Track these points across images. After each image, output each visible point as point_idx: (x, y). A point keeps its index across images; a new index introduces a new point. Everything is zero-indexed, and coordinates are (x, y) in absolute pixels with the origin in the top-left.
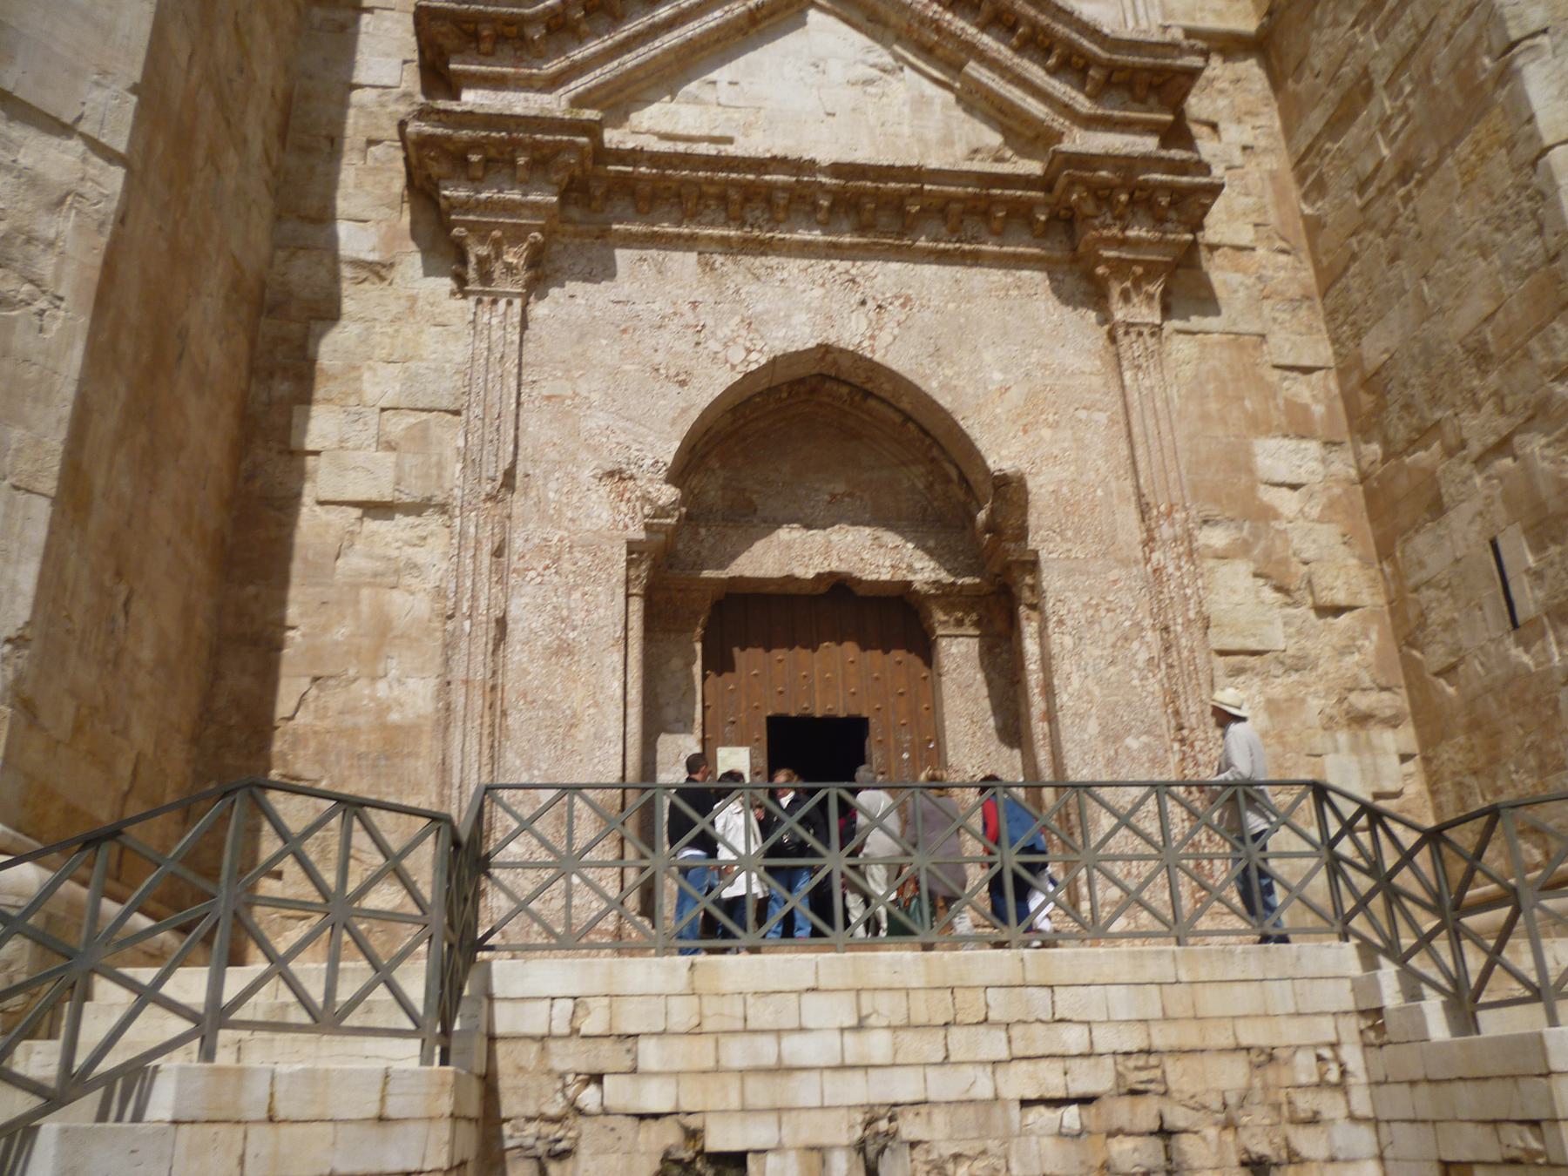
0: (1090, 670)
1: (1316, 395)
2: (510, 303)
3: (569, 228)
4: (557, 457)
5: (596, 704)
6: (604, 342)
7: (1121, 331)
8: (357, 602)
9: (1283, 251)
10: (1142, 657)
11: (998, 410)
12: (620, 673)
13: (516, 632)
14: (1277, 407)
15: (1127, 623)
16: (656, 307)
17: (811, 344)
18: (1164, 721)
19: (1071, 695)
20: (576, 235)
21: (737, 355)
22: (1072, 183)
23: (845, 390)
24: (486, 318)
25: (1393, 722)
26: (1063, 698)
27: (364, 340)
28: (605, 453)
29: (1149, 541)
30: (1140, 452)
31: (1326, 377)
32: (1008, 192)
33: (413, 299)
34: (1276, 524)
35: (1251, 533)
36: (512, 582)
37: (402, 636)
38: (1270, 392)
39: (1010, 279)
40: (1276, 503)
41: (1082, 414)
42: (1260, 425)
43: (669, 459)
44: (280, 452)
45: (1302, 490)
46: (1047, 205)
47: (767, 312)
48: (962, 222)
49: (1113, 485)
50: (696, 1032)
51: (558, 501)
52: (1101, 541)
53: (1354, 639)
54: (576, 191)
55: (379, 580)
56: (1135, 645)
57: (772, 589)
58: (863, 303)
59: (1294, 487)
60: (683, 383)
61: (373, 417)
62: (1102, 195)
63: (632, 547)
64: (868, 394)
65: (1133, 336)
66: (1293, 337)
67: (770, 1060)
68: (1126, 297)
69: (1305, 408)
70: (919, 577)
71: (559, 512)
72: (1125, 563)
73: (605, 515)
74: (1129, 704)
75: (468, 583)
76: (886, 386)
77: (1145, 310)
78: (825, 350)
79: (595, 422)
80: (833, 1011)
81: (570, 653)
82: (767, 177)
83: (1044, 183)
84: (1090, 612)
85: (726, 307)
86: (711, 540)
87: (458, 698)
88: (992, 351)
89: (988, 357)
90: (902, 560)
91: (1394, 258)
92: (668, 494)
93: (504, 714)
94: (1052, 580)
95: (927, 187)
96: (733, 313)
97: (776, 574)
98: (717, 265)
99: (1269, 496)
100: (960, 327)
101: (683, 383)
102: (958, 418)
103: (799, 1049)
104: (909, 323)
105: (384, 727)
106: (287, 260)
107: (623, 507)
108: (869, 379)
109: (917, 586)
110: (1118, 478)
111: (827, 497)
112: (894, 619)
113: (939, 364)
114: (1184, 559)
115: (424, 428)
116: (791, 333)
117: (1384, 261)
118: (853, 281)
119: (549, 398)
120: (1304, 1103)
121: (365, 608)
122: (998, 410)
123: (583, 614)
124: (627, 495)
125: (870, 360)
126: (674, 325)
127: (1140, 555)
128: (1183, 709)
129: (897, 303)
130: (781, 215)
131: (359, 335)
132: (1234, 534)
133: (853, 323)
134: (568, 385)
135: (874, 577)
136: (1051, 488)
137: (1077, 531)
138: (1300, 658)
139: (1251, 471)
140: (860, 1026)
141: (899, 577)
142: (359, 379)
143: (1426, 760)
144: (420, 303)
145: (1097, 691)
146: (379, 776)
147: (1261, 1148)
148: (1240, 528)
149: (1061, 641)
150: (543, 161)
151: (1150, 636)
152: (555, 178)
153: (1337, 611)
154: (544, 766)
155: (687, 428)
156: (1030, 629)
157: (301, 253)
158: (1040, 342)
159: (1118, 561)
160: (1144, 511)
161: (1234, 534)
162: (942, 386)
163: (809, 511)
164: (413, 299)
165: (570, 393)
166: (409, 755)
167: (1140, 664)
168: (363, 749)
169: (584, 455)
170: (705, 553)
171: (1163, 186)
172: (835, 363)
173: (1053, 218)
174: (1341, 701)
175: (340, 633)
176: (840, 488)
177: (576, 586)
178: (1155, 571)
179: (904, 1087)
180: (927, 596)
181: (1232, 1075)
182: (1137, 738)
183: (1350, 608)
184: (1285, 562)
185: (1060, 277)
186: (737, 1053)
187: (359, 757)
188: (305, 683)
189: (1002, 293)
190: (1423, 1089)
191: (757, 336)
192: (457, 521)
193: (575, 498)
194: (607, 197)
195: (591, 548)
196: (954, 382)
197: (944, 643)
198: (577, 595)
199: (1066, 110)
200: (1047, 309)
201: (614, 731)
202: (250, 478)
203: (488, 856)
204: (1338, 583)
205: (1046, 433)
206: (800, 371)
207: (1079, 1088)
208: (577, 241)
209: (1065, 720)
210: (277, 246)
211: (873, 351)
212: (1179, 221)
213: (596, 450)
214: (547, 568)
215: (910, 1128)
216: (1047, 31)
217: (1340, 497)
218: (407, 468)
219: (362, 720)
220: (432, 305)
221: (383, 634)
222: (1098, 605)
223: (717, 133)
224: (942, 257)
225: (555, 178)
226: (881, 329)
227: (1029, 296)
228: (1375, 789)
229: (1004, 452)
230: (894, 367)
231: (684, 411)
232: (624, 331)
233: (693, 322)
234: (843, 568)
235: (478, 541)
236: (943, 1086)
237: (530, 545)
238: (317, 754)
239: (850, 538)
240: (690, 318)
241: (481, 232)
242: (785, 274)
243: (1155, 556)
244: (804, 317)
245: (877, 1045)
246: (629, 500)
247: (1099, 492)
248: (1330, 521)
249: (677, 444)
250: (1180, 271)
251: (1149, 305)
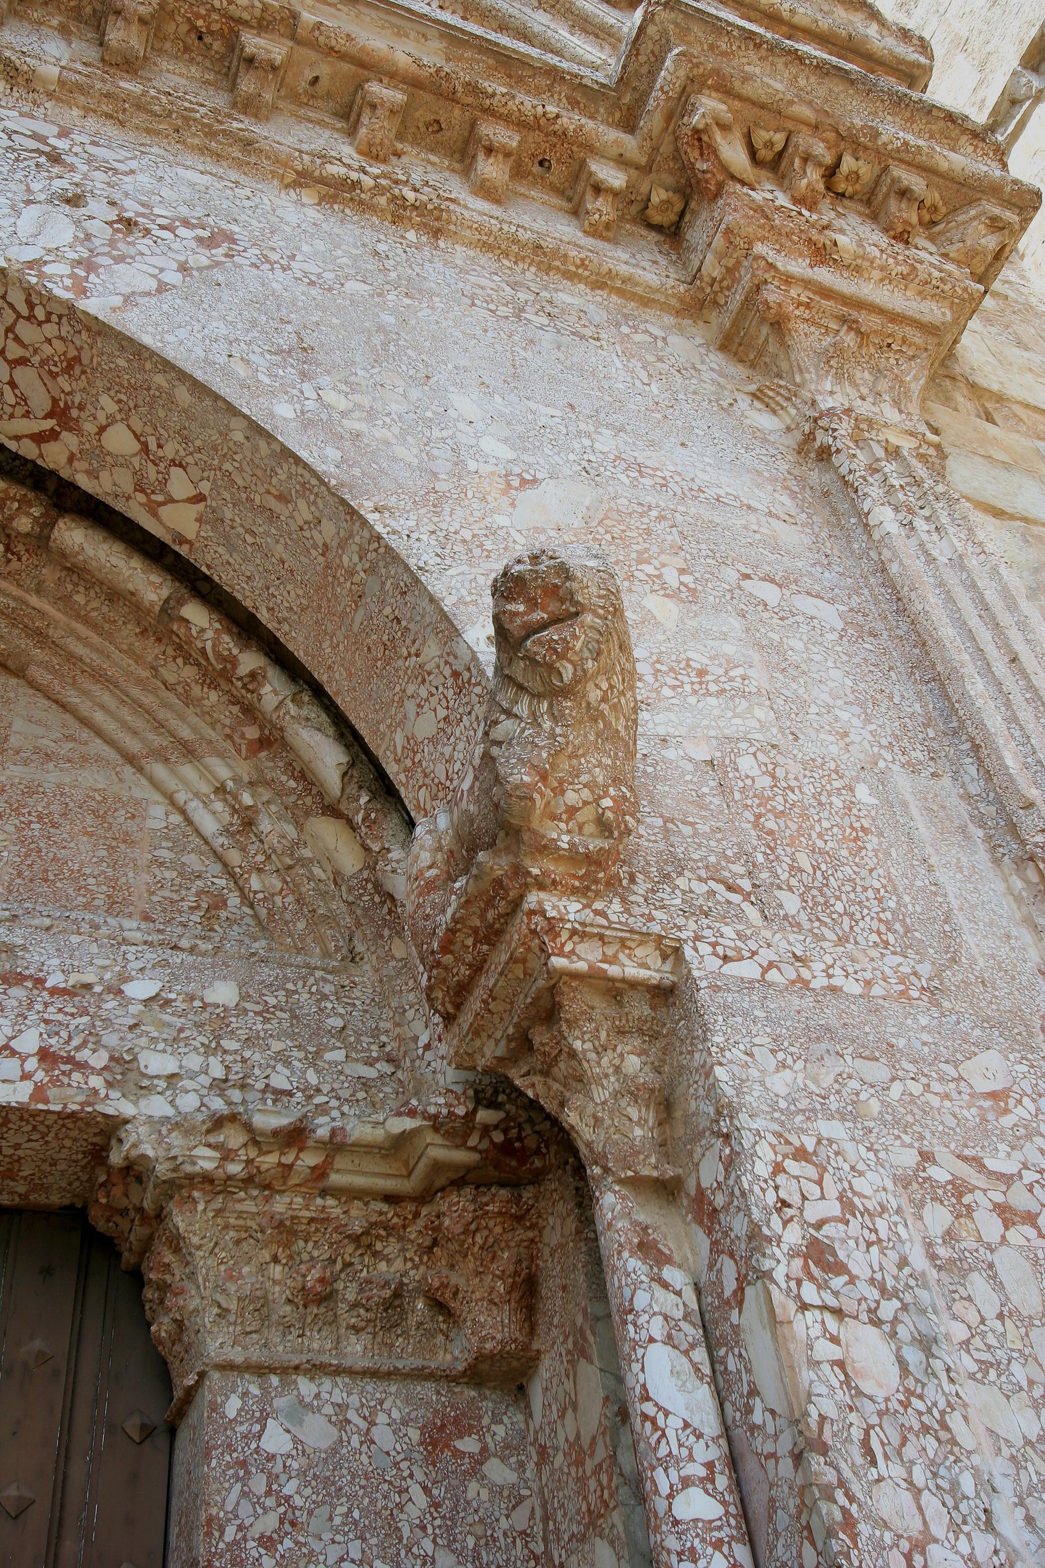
11: (501, 520)
70: (158, 1106)
90: (93, 1039)
94: (752, 1069)
100: (380, 329)
102: (365, 507)
108: (61, 413)
109: (141, 1142)
110: (913, 768)
125: (70, 312)
136: (702, 753)
137: (816, 899)
141: (67, 1097)
149: (836, 1358)
156: (655, 1302)
162: (306, 422)
180: (185, 1184)
222: (958, 1188)
226: (120, 259)
247: (862, 792)
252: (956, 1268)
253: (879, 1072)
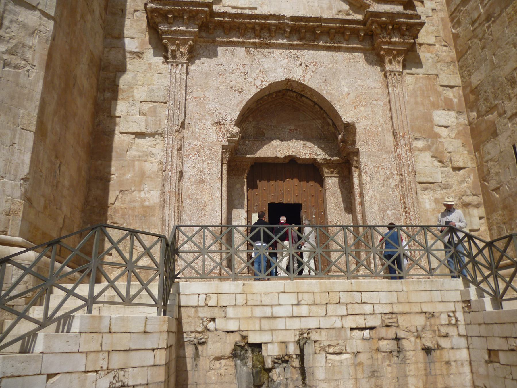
0: (375, 188)
1: (454, 96)
2: (182, 66)
3: (202, 40)
4: (199, 117)
5: (212, 199)
6: (214, 79)
7: (388, 74)
8: (134, 166)
9: (445, 46)
10: (393, 184)
11: (346, 101)
12: (220, 189)
13: (186, 176)
14: (441, 100)
15: (388, 173)
16: (231, 66)
17: (283, 79)
18: (400, 206)
19: (369, 197)
20: (204, 42)
21: (258, 83)
22: (373, 22)
23: (294, 94)
24: (174, 71)
25: (477, 206)
26: (366, 198)
27: (134, 78)
28: (215, 116)
29: (396, 145)
30: (394, 115)
31: (458, 90)
32: (350, 26)
33: (150, 64)
34: (440, 140)
35: (431, 143)
36: (184, 159)
37: (148, 177)
38: (439, 94)
39: (351, 56)
40: (440, 132)
41: (375, 102)
42: (435, 106)
43: (236, 118)
44: (108, 117)
45: (449, 128)
46: (364, 30)
47: (268, 68)
48: (335, 36)
49: (385, 126)
50: (245, 305)
51: (199, 132)
52: (380, 145)
53: (465, 178)
54: (204, 27)
55: (141, 159)
56: (391, 180)
57: (270, 161)
58: (301, 65)
59: (446, 127)
60: (240, 92)
61: (138, 104)
62: (383, 27)
63: (224, 147)
64: (302, 96)
65: (393, 75)
66: (447, 76)
67: (269, 314)
68: (390, 62)
69: (451, 100)
70: (319, 157)
71: (199, 136)
72: (388, 153)
73: (214, 137)
74: (388, 200)
75: (170, 160)
76: (309, 93)
77: (397, 66)
78: (288, 81)
79: (211, 106)
80: (289, 299)
81: (204, 183)
82: (269, 21)
83: (363, 22)
84: (376, 169)
85: (255, 66)
86: (250, 145)
87: (167, 197)
88: (344, 80)
89: (343, 83)
90: (313, 151)
91: (483, 48)
92: (235, 130)
93: (182, 202)
94: (363, 158)
95: (323, 24)
96: (257, 68)
97: (271, 156)
98: (252, 52)
99: (438, 130)
100: (334, 73)
101: (240, 92)
102: (333, 104)
103: (278, 311)
104: (316, 71)
105: (143, 207)
106: (108, 52)
107: (221, 134)
108: (303, 91)
109: (318, 160)
110: (386, 124)
111: (288, 131)
112: (310, 171)
113: (326, 85)
114: (408, 151)
115: (155, 108)
116: (276, 75)
117: (480, 49)
118: (298, 57)
119: (196, 98)
120: (444, 330)
121: (136, 168)
122: (346, 101)
123: (208, 170)
124: (222, 130)
125: (303, 84)
126: (237, 73)
127: (393, 150)
128: (406, 202)
129: (312, 65)
130: (273, 35)
131: (133, 77)
132: (425, 143)
133: (297, 72)
134: (202, 93)
135: (304, 157)
137: (372, 142)
138: (446, 185)
139: (432, 122)
140: (298, 304)
141: (312, 157)
142: (133, 92)
143: (488, 219)
144: (153, 66)
145: (378, 195)
146: (142, 222)
147: (429, 344)
148: (427, 141)
149: (366, 179)
150: (193, 17)
151: (396, 177)
152: (197, 22)
153: (460, 169)
154: (195, 220)
155: (242, 108)
156: (356, 175)
157: (113, 49)
158: (361, 77)
159: (385, 152)
160: (395, 135)
161: (425, 143)
162: (327, 93)
163: (282, 135)
164: (150, 64)
165: (203, 96)
166: (152, 216)
167: (392, 186)
168: (137, 214)
169: (207, 117)
170: (248, 149)
171: (404, 23)
172: (291, 85)
173: (366, 34)
174: (460, 199)
175: (129, 176)
176: (293, 127)
177: (205, 160)
178: (398, 155)
179: (312, 323)
181: (420, 321)
182: (391, 211)
183: (464, 168)
184: (442, 152)
185: (368, 55)
186: (258, 312)
187: (136, 216)
188: (118, 192)
189: (348, 61)
190: (483, 326)
191: (265, 76)
192: (166, 139)
193: (205, 131)
194: (214, 29)
195: (210, 148)
196: (331, 92)
197: (327, 179)
198: (205, 163)
200: (363, 66)
201: (218, 208)
202: (98, 125)
203: (178, 249)
204: (460, 160)
205: (362, 109)
206: (279, 88)
207: (369, 325)
208: (205, 44)
209: (367, 205)
210: (105, 47)
211: (304, 81)
212: (409, 36)
213: (211, 115)
214: (196, 154)
215: (314, 336)
217: (462, 130)
218: (149, 121)
219: (136, 205)
220: (156, 66)
221: (142, 176)
223: (251, 6)
225: (197, 22)
227: (357, 62)
228: (470, 228)
229: (348, 115)
230: (311, 87)
231: (241, 102)
232: (221, 75)
233: (244, 72)
234: (294, 154)
235: (173, 146)
236: (325, 323)
237: (190, 147)
238: (122, 215)
239: (296, 144)
240: (243, 70)
241: (172, 41)
242: (275, 55)
243: (398, 150)
244: (281, 70)
245: (304, 310)
246: (222, 132)
247: (380, 129)
248: (458, 139)
249: (238, 113)
250: (409, 53)
251: (398, 65)
252: (376, 173)
253: (374, 158)
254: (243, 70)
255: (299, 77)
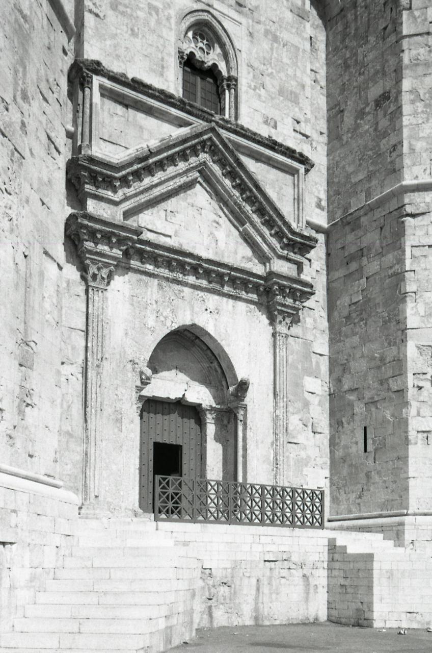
7: (278, 335)
46: (264, 286)
57: (157, 399)
62: (282, 288)
83: (265, 279)
88: (238, 329)
95: (232, 273)
143: (330, 479)
150: (121, 241)
199: (273, 250)
216: (274, 221)
224: (229, 296)
241: (94, 262)
254: (155, 306)
255: (204, 323)
